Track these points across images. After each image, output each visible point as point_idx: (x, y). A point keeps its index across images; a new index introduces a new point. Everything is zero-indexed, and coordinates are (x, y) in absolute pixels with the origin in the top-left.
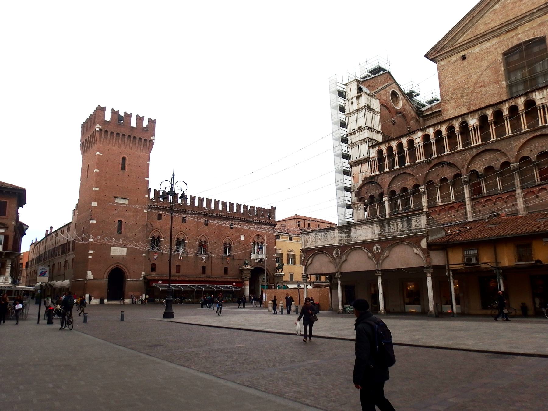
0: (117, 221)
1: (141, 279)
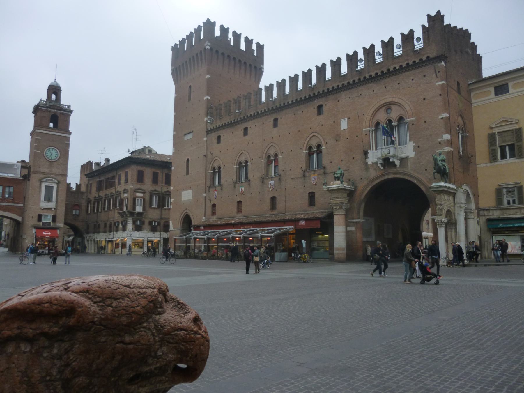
0: (186, 161)
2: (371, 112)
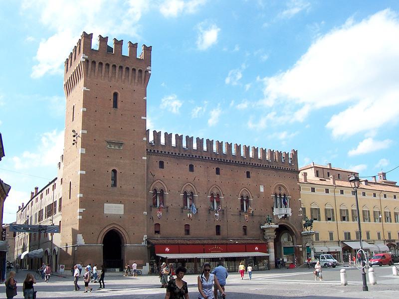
1: (143, 244)
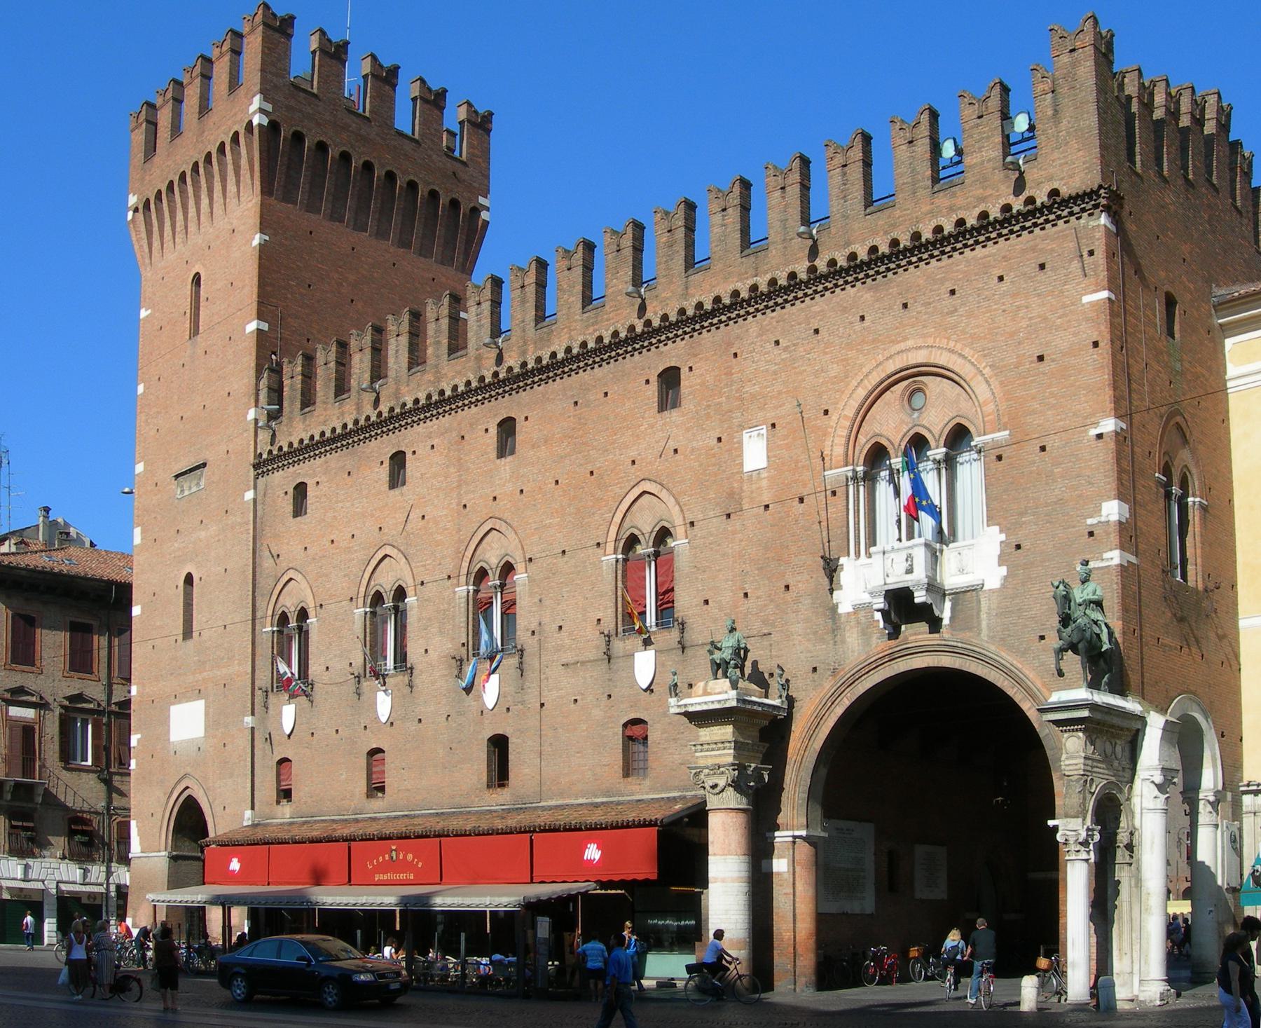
0: (181, 583)
2: (855, 404)
